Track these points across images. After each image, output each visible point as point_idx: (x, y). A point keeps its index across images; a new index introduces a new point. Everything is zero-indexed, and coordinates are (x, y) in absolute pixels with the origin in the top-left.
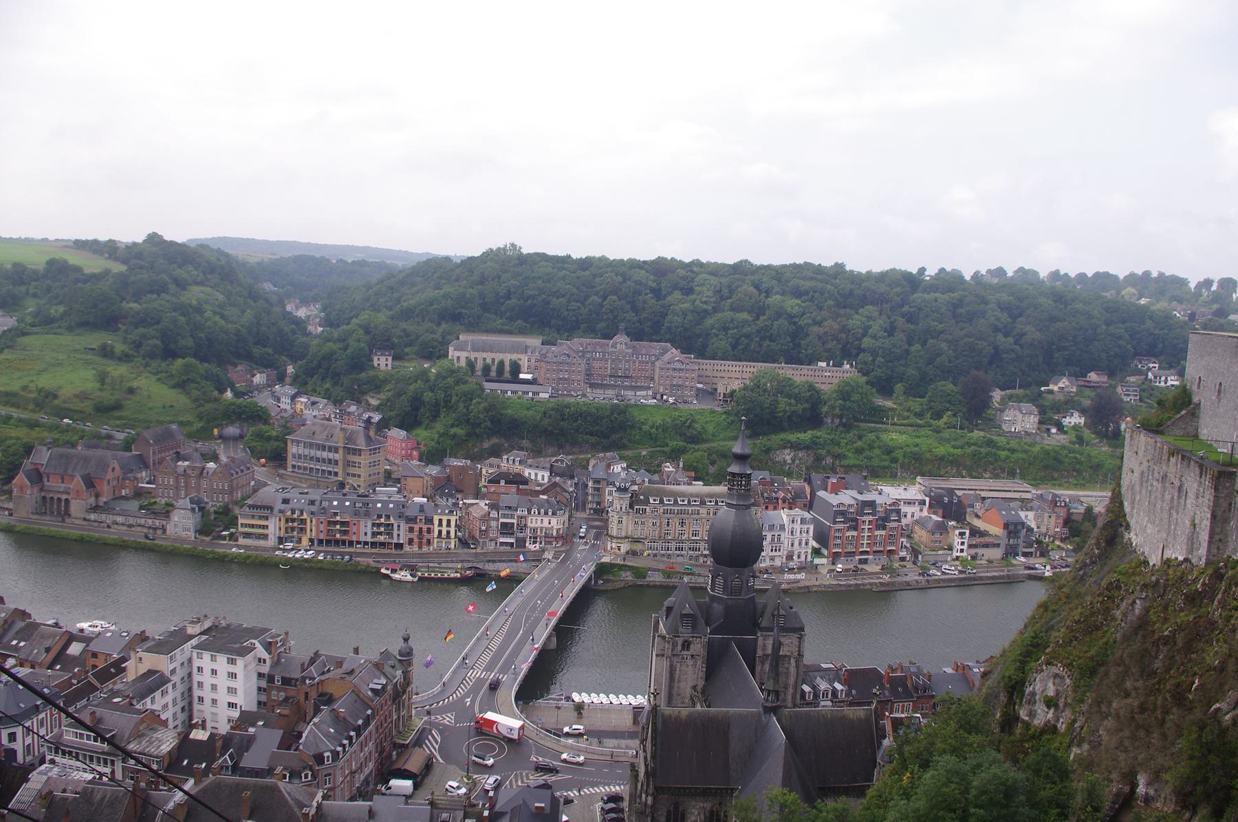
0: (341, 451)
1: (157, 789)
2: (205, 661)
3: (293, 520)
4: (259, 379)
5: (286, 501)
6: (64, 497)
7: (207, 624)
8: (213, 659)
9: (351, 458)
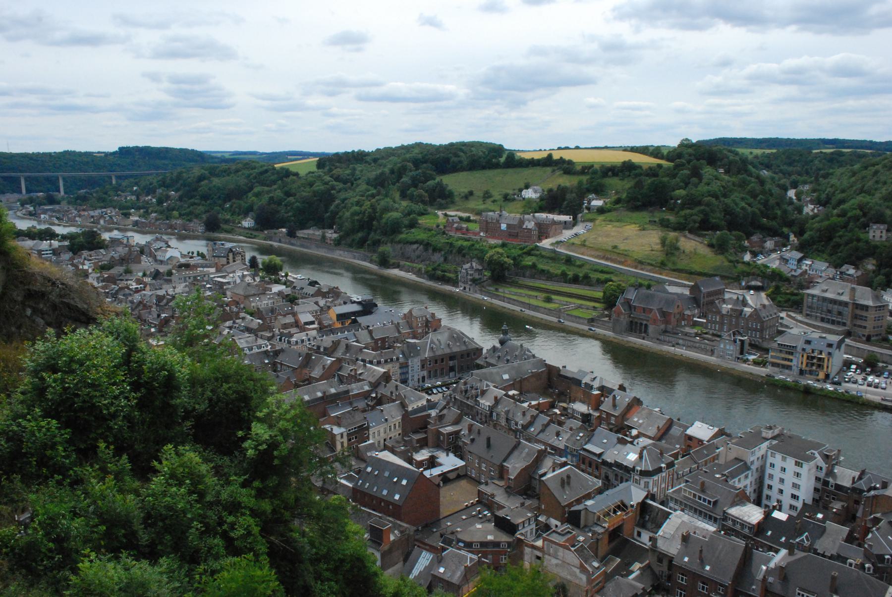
0: (850, 306)
1: (757, 549)
2: (777, 459)
3: (813, 358)
4: (769, 244)
5: (808, 342)
6: (645, 322)
7: (776, 432)
8: (784, 459)
9: (859, 312)
